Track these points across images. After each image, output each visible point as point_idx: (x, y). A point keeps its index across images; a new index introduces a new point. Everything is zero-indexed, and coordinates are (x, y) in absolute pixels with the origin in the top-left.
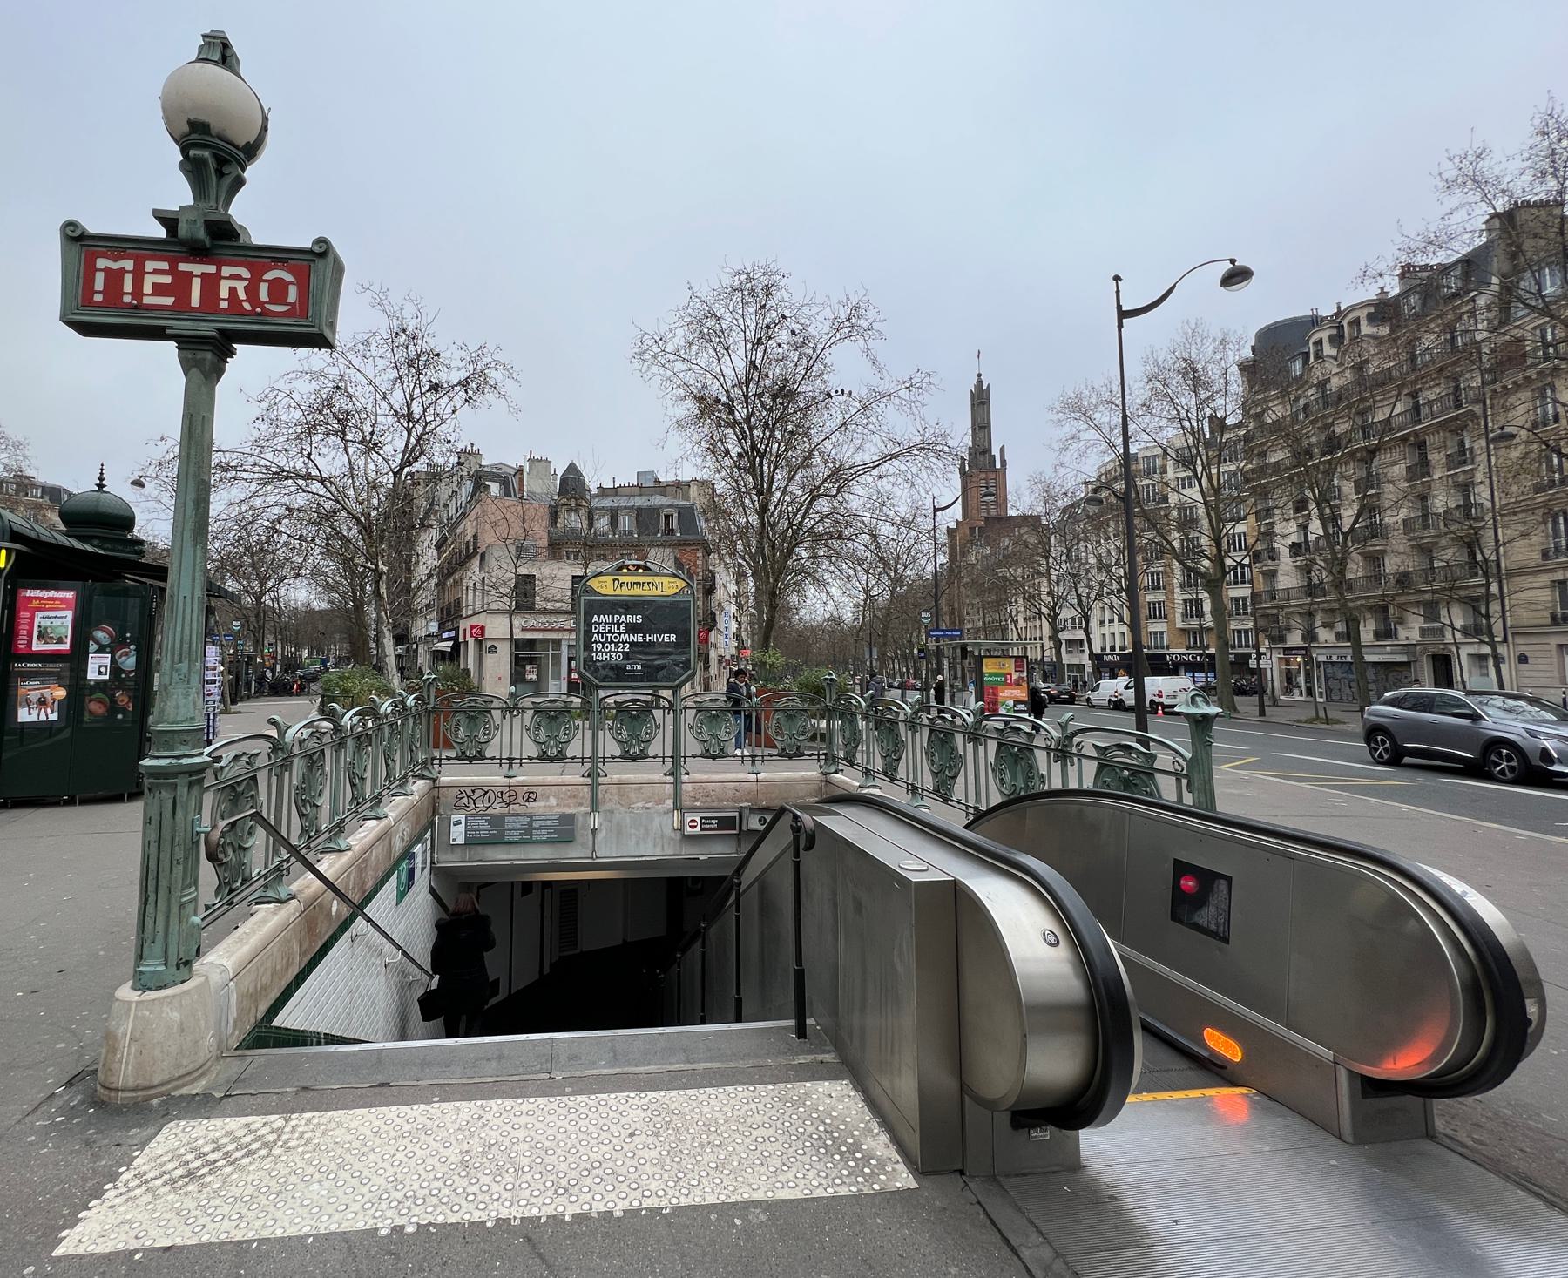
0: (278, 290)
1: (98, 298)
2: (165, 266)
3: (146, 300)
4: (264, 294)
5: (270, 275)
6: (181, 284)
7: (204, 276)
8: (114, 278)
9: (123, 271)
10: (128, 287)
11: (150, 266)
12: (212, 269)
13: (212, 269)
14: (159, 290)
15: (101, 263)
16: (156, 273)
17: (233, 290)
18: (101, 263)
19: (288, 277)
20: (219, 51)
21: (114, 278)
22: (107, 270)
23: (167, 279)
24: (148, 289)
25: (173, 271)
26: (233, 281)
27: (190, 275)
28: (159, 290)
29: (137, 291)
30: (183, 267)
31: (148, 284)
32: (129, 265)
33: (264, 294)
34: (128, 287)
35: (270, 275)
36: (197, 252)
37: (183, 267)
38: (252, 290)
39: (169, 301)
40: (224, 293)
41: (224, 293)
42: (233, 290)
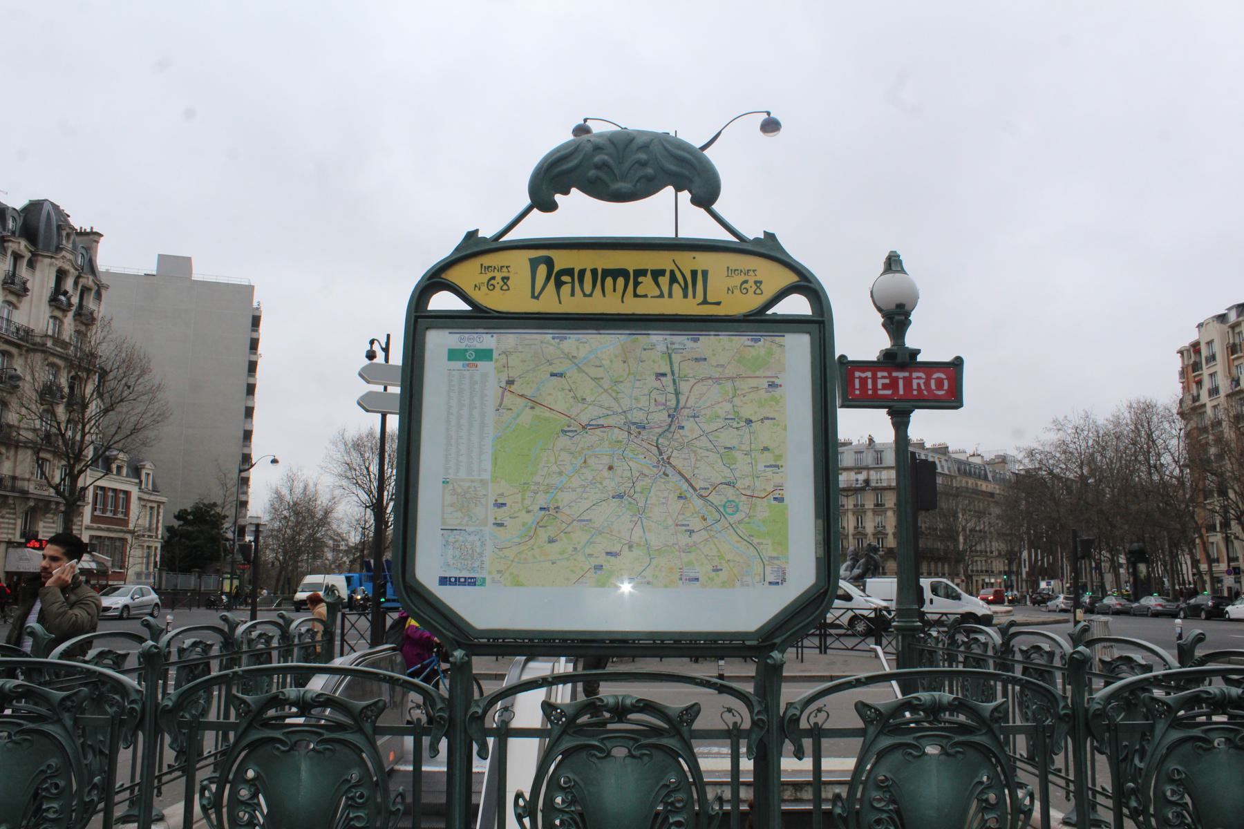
0: (940, 384)
1: (857, 392)
2: (886, 374)
3: (880, 392)
4: (933, 386)
5: (935, 376)
6: (893, 384)
7: (904, 378)
8: (863, 381)
9: (867, 378)
10: (870, 386)
11: (880, 374)
12: (907, 374)
13: (907, 374)
14: (885, 387)
15: (857, 374)
16: (883, 378)
17: (919, 384)
18: (857, 374)
19: (943, 376)
20: (893, 263)
21: (863, 381)
22: (860, 378)
23: (887, 381)
24: (880, 386)
25: (890, 377)
26: (918, 379)
27: (897, 378)
28: (885, 387)
29: (875, 388)
30: (894, 374)
31: (880, 382)
32: (869, 374)
33: (933, 386)
34: (870, 386)
35: (935, 376)
36: (902, 367)
37: (894, 374)
38: (927, 384)
39: (889, 392)
40: (915, 387)
41: (915, 387)
42: (919, 384)
